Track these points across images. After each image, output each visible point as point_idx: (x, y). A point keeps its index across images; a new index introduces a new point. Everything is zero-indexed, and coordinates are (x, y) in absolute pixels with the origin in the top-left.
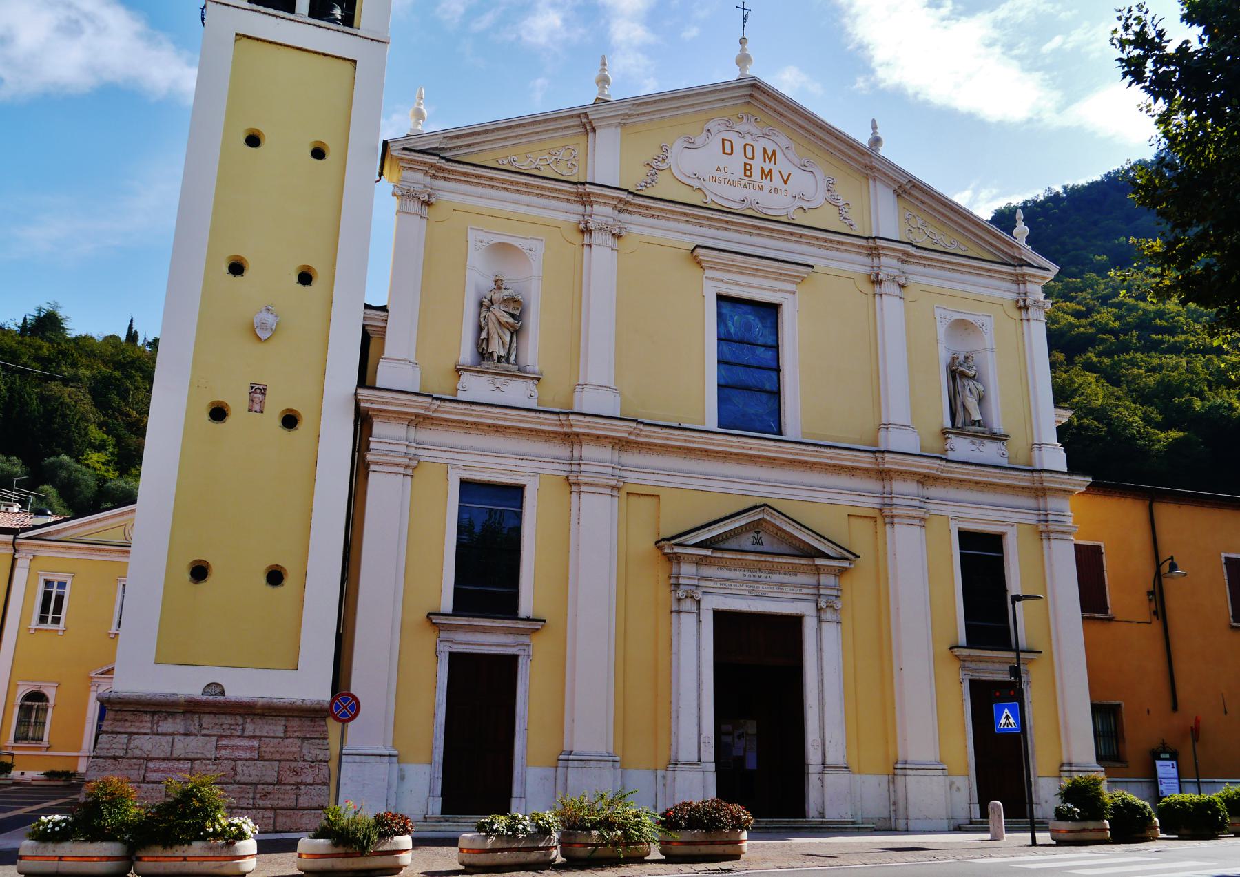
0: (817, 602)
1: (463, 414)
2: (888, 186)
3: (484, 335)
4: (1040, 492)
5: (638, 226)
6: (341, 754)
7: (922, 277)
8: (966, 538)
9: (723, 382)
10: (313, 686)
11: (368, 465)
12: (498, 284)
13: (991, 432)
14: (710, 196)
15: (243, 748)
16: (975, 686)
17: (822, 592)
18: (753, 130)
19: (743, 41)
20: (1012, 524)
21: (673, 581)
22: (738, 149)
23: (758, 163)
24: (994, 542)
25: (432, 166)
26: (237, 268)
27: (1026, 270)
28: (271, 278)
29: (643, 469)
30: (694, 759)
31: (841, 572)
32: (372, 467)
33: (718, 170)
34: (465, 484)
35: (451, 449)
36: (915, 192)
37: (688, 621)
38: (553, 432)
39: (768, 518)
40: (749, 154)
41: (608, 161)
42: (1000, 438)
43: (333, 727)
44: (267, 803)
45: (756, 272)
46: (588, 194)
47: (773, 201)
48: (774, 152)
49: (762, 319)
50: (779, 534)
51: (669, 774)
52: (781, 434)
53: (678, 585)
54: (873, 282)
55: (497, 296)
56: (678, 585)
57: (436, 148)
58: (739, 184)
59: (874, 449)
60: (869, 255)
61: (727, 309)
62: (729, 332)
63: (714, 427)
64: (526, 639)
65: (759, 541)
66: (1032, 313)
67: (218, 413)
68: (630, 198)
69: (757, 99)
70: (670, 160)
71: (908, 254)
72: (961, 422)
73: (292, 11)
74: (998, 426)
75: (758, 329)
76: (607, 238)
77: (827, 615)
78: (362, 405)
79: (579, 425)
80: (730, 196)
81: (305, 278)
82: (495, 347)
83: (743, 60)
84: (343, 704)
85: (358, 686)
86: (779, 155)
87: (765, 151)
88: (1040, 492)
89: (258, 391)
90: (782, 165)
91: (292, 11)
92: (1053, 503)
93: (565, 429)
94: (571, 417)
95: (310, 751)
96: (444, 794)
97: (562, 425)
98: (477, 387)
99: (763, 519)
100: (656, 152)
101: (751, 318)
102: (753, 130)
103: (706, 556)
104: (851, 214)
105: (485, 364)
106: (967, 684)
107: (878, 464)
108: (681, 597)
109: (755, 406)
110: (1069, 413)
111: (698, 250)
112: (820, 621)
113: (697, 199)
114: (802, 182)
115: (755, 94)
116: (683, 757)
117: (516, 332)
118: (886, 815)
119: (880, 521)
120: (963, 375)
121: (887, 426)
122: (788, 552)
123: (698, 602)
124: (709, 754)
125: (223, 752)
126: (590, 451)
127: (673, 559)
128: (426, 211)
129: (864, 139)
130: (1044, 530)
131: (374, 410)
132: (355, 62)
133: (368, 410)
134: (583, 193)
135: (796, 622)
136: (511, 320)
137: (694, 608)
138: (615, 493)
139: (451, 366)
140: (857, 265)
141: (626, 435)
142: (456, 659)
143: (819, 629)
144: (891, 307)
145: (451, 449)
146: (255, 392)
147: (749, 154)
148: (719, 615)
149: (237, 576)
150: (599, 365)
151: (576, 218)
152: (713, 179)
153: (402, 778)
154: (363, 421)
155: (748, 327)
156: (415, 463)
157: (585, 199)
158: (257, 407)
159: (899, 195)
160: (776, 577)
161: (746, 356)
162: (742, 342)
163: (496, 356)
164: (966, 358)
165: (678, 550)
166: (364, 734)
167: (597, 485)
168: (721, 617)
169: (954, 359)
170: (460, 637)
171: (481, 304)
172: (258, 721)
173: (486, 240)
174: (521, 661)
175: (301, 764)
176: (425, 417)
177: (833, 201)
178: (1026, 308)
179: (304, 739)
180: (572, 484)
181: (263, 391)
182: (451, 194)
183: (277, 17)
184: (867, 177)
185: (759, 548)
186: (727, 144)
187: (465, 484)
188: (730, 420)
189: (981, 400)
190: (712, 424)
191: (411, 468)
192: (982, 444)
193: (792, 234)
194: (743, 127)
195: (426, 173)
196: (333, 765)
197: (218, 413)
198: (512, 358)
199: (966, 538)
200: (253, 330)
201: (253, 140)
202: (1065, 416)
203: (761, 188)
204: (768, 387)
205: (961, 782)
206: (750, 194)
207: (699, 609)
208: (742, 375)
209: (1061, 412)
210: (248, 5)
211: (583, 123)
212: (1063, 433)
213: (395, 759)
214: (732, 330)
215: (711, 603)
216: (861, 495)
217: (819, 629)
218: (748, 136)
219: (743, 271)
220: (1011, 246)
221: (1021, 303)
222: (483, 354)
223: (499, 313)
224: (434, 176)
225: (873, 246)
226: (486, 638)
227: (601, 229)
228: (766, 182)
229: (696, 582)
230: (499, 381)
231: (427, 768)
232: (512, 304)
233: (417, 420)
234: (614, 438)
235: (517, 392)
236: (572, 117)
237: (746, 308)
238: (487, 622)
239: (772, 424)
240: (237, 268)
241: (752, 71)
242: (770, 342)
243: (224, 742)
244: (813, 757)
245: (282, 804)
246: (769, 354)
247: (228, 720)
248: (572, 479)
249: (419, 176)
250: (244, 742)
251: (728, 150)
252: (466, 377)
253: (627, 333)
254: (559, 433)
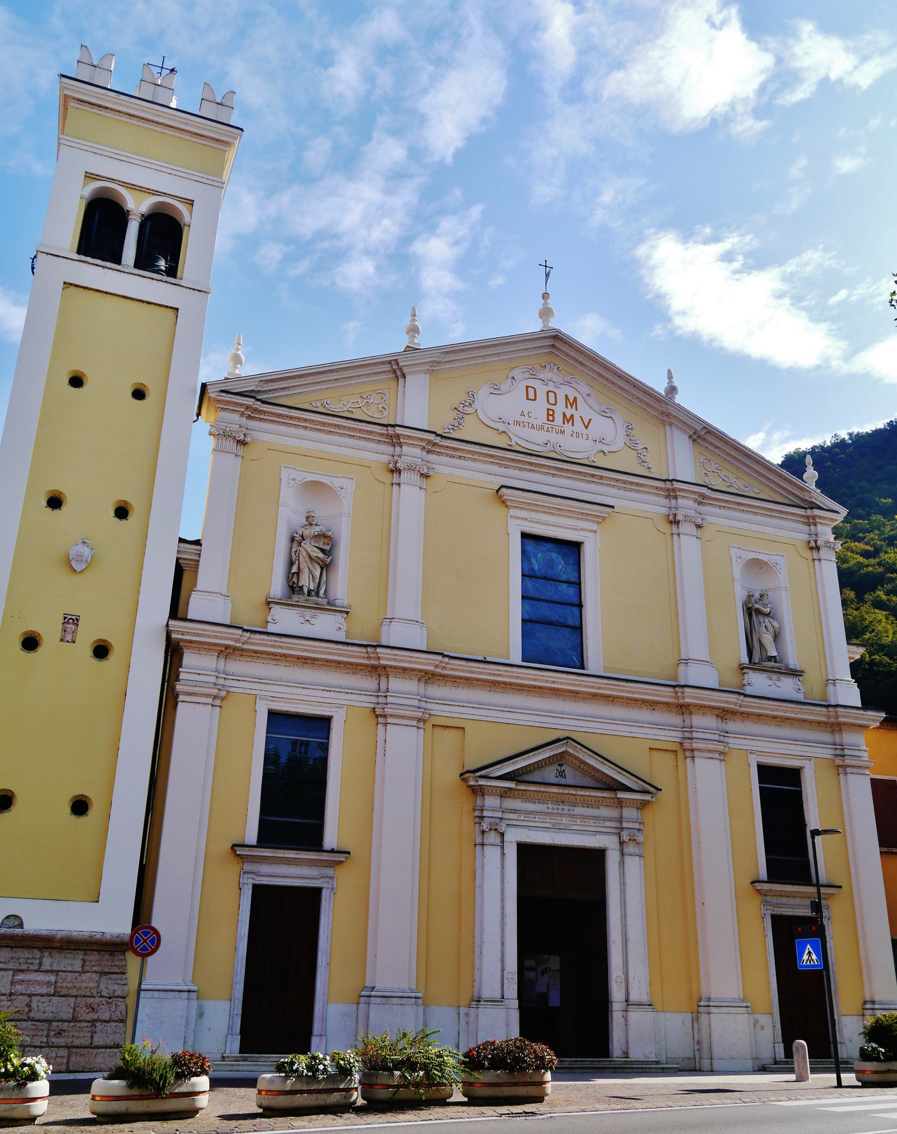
0: (619, 835)
1: (273, 646)
2: (684, 431)
3: (294, 569)
4: (836, 727)
5: (445, 467)
6: (139, 990)
7: (719, 519)
8: (766, 772)
9: (527, 617)
10: (113, 919)
11: (178, 695)
12: (310, 521)
13: (787, 668)
14: (515, 439)
15: (40, 983)
16: (775, 919)
17: (625, 825)
18: (555, 378)
19: (545, 296)
20: (809, 758)
21: (477, 813)
22: (541, 394)
23: (560, 408)
24: (793, 776)
25: (248, 407)
26: (55, 502)
27: (817, 512)
28: (88, 511)
29: (449, 702)
30: (497, 995)
31: (644, 805)
32: (181, 698)
33: (522, 414)
35: (260, 680)
36: (708, 437)
37: (492, 854)
38: (361, 665)
39: (571, 751)
40: (552, 401)
41: (416, 405)
42: (795, 673)
43: (132, 961)
44: (61, 1041)
45: (559, 512)
46: (398, 436)
48: (575, 399)
49: (564, 556)
50: (583, 767)
51: (472, 1011)
52: (583, 668)
53: (482, 818)
54: (671, 522)
55: (308, 532)
56: (482, 818)
57: (253, 391)
58: (542, 428)
59: (674, 683)
60: (667, 497)
61: (531, 546)
62: (533, 569)
63: (518, 660)
64: (330, 872)
65: (562, 774)
66: (824, 553)
67: (31, 643)
68: (438, 440)
69: (559, 349)
70: (476, 405)
71: (704, 496)
72: (759, 659)
73: (119, 262)
74: (793, 661)
75: (561, 566)
76: (416, 477)
77: (630, 848)
78: (174, 636)
79: (386, 658)
80: (534, 439)
81: (122, 512)
82: (306, 581)
83: (546, 313)
84: (144, 937)
85: (158, 921)
86: (580, 401)
87: (567, 397)
88: (836, 727)
89: (71, 621)
90: (583, 411)
91: (119, 262)
92: (848, 738)
93: (372, 661)
94: (379, 650)
95: (108, 986)
96: (242, 1032)
97: (369, 658)
98: (287, 620)
99: (566, 752)
100: (463, 397)
101: (554, 555)
102: (555, 378)
103: (510, 789)
105: (295, 598)
106: (768, 920)
107: (677, 698)
108: (485, 829)
109: (558, 640)
110: (862, 650)
111: (504, 490)
112: (622, 854)
113: (502, 442)
114: (602, 427)
115: (556, 346)
116: (486, 994)
117: (326, 567)
118: (690, 1054)
119: (680, 755)
120: (759, 612)
121: (686, 661)
122: (590, 785)
123: (502, 835)
124: (512, 991)
125: (19, 988)
126: (396, 684)
127: (477, 791)
128: (241, 450)
129: (660, 387)
130: (841, 764)
131: (185, 641)
132: (177, 309)
133: (178, 641)
134: (393, 434)
135: (598, 856)
136: (321, 555)
137: (498, 841)
138: (421, 725)
139: (262, 599)
140: (654, 506)
141: (432, 668)
142: (258, 890)
143: (622, 863)
144: (689, 546)
145: (260, 680)
146: (68, 623)
147: (552, 401)
148: (523, 849)
150: (406, 600)
151: (386, 459)
152: (518, 423)
153: (201, 1015)
154: (174, 652)
155: (551, 564)
156: (223, 694)
157: (395, 441)
158: (69, 638)
159: (694, 440)
160: (579, 810)
161: (549, 591)
162: (545, 578)
163: (306, 590)
164: (762, 596)
165: (482, 782)
166: (163, 969)
167: (403, 717)
168: (523, 849)
169: (750, 596)
170: (264, 868)
171: (292, 539)
172: (56, 955)
173: (299, 478)
174: (325, 894)
175: (98, 1000)
176: (235, 649)
177: (632, 444)
178: (818, 548)
179: (102, 973)
180: (379, 716)
181: (76, 621)
182: (267, 435)
183: (104, 267)
184: (663, 423)
185: (562, 781)
186: (531, 391)
189: (777, 636)
190: (516, 657)
191: (219, 698)
192: (778, 680)
193: (593, 476)
194: (546, 375)
195: (242, 414)
196: (131, 1001)
197: (31, 643)
198: (322, 592)
199: (766, 772)
200: (69, 562)
201: (76, 381)
202: (858, 652)
203: (563, 432)
204: (571, 622)
205: (765, 1020)
206: (553, 437)
207: (503, 842)
208: (545, 611)
209: (854, 648)
210: (76, 257)
211: (394, 369)
212: (856, 668)
213: (194, 995)
214: (536, 567)
215: (515, 836)
216: (663, 729)
217: (622, 863)
218: (551, 383)
219: (547, 511)
220: (802, 489)
221: (813, 544)
222: (293, 588)
223: (310, 548)
224: (249, 417)
225: (670, 489)
226: (289, 870)
227: (410, 468)
228: (568, 427)
229: (499, 815)
230: (308, 613)
231: (226, 1005)
232: (323, 540)
233: (227, 652)
234: (420, 671)
235: (325, 625)
236: (383, 363)
237: (549, 546)
238: (291, 854)
239: (574, 658)
240: (55, 502)
241: (555, 323)
242: (572, 579)
243: (21, 977)
244: (617, 993)
245: (77, 1042)
246: (572, 591)
247: (26, 954)
248: (378, 711)
249: (236, 417)
250: (41, 977)
251: (531, 396)
252: (276, 610)
253: (435, 569)
254: (366, 666)
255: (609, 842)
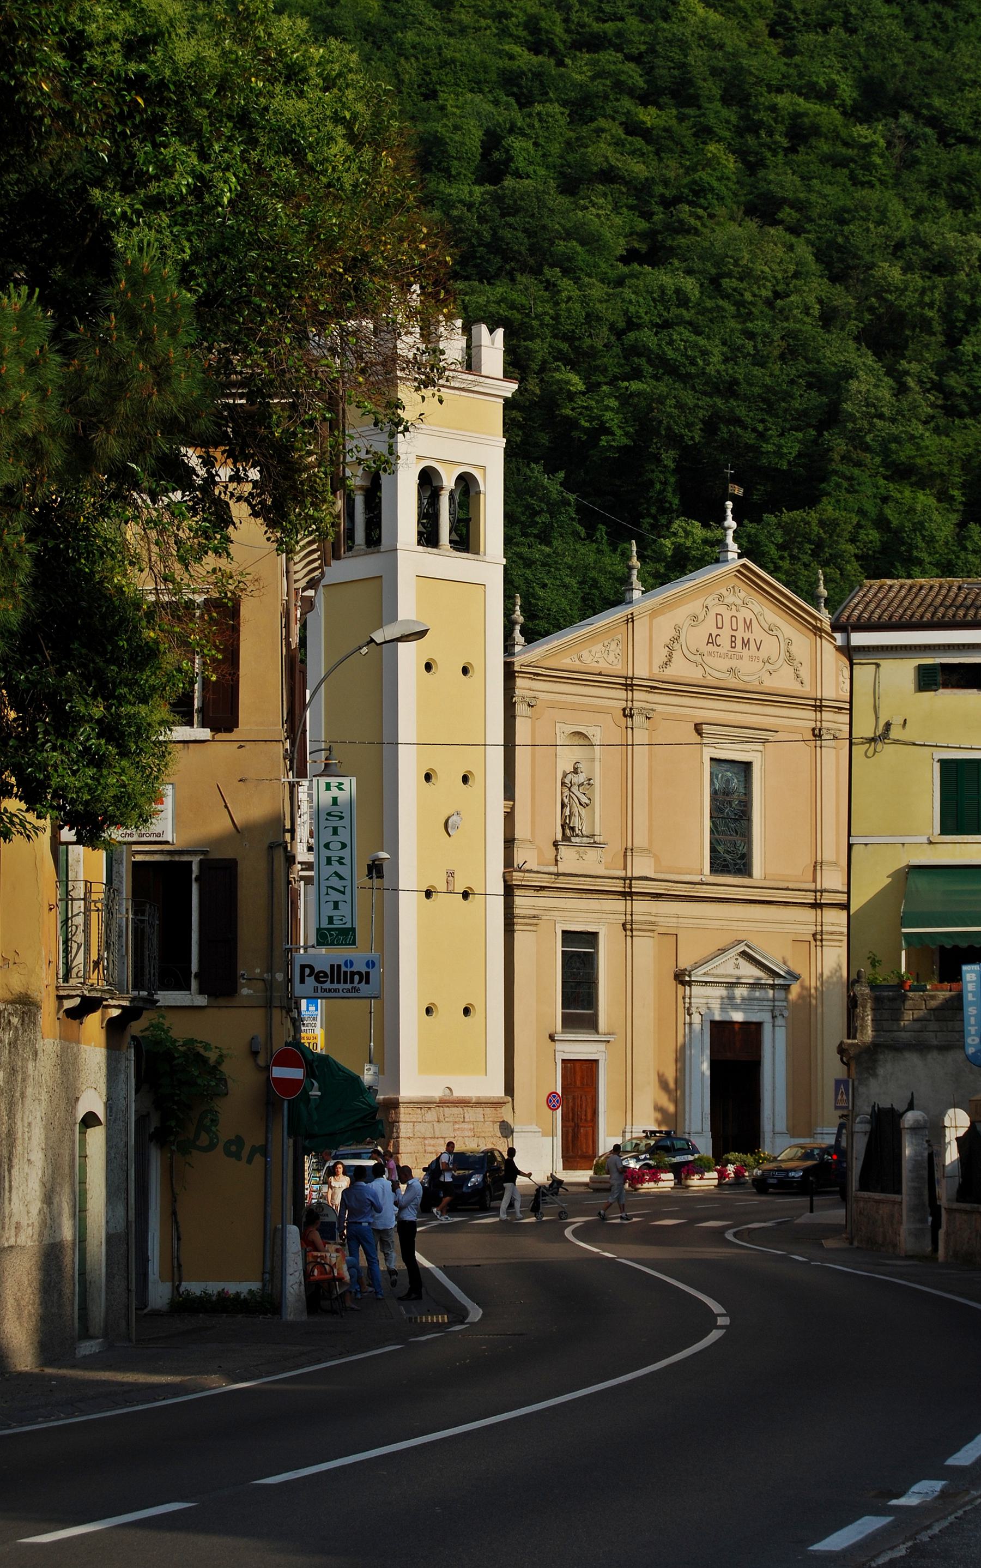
23: (739, 635)
34: (564, 932)
47: (750, 672)
70: (682, 639)
86: (754, 622)
90: (757, 633)
100: (673, 633)
102: (739, 602)
104: (805, 673)
114: (771, 647)
119: (813, 943)
149: (450, 1011)
154: (509, 891)
171: (563, 784)
181: (452, 874)
187: (564, 932)
188: (719, 865)
206: (734, 663)
237: (726, 766)
243: (457, 1126)
250: (465, 1126)
255: (765, 1017)
